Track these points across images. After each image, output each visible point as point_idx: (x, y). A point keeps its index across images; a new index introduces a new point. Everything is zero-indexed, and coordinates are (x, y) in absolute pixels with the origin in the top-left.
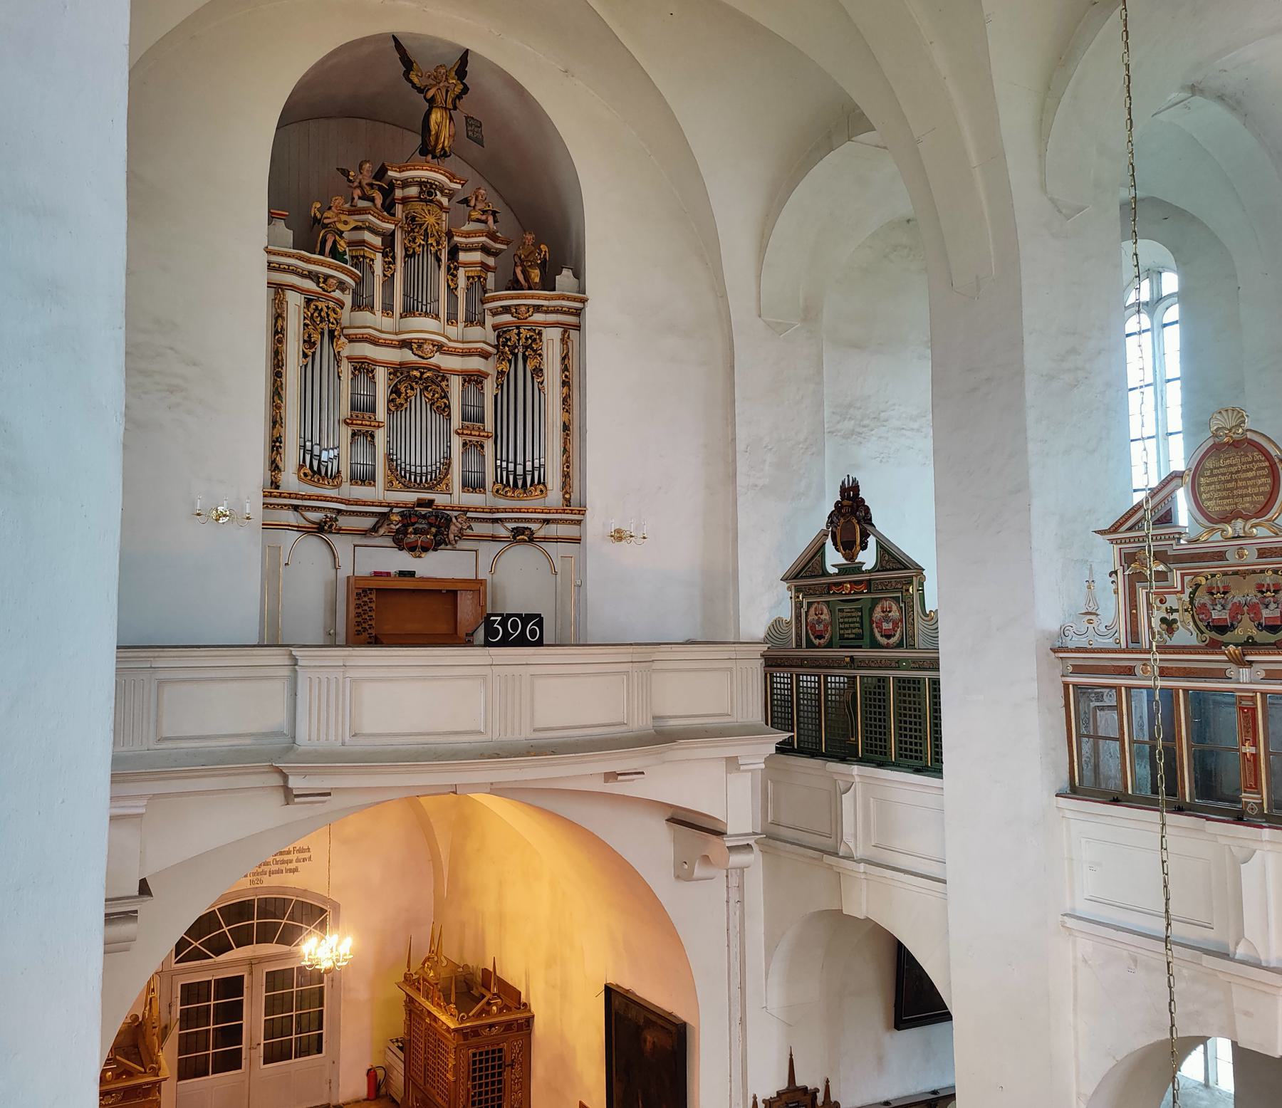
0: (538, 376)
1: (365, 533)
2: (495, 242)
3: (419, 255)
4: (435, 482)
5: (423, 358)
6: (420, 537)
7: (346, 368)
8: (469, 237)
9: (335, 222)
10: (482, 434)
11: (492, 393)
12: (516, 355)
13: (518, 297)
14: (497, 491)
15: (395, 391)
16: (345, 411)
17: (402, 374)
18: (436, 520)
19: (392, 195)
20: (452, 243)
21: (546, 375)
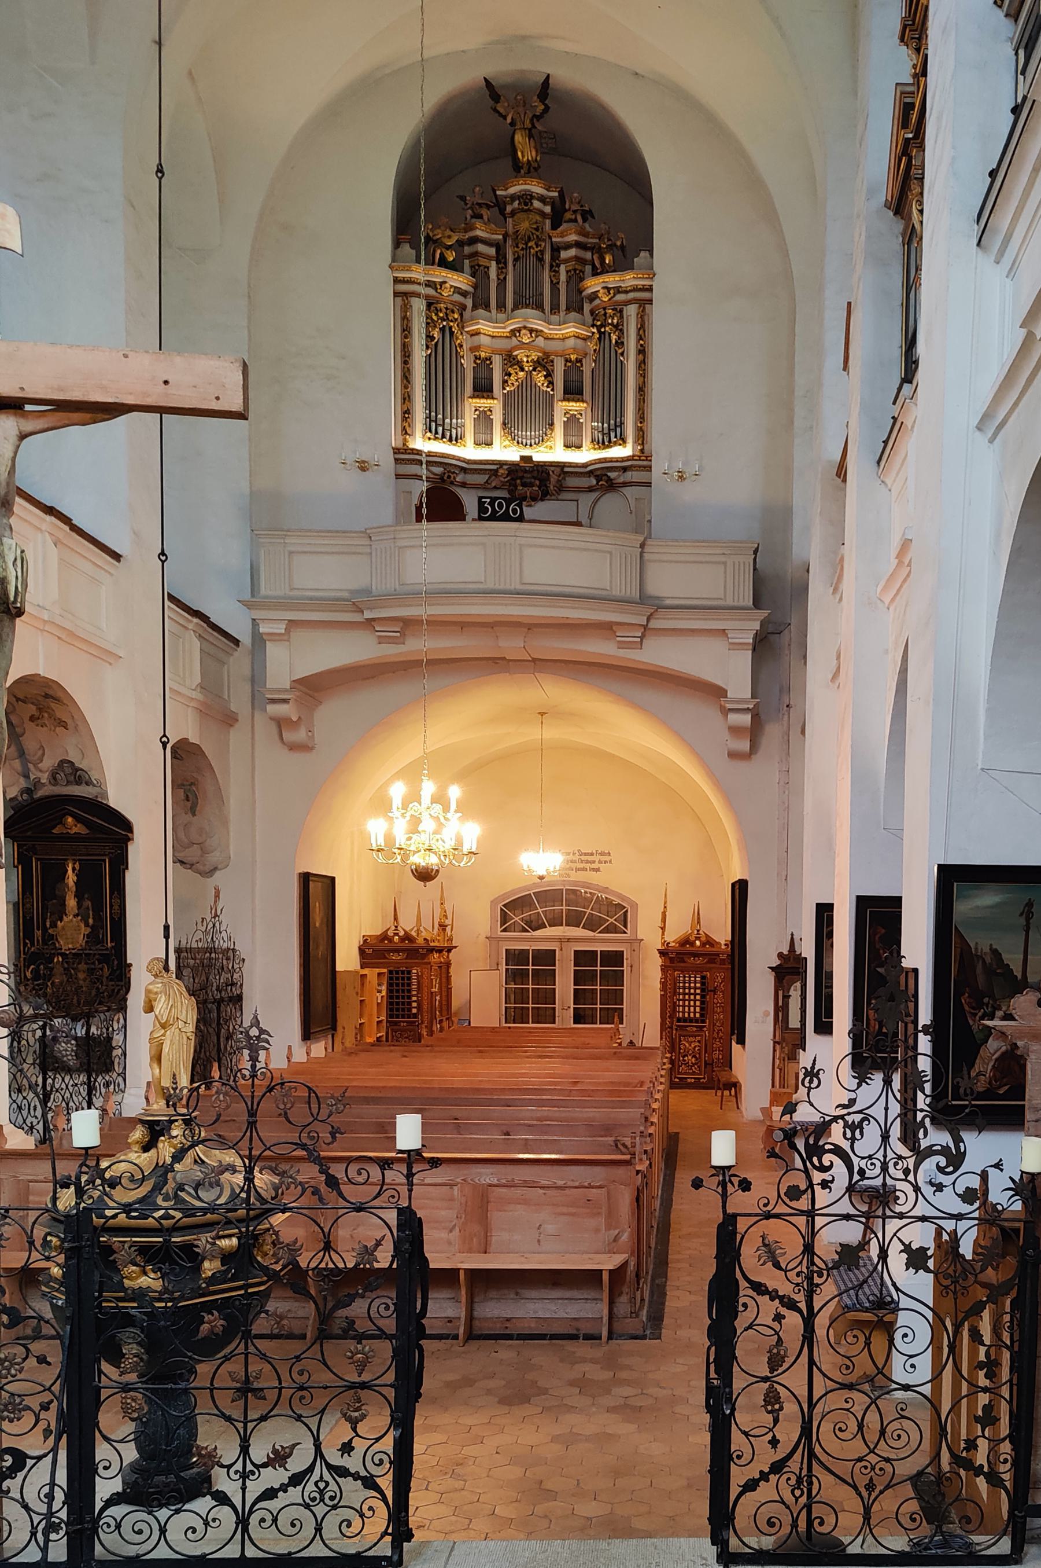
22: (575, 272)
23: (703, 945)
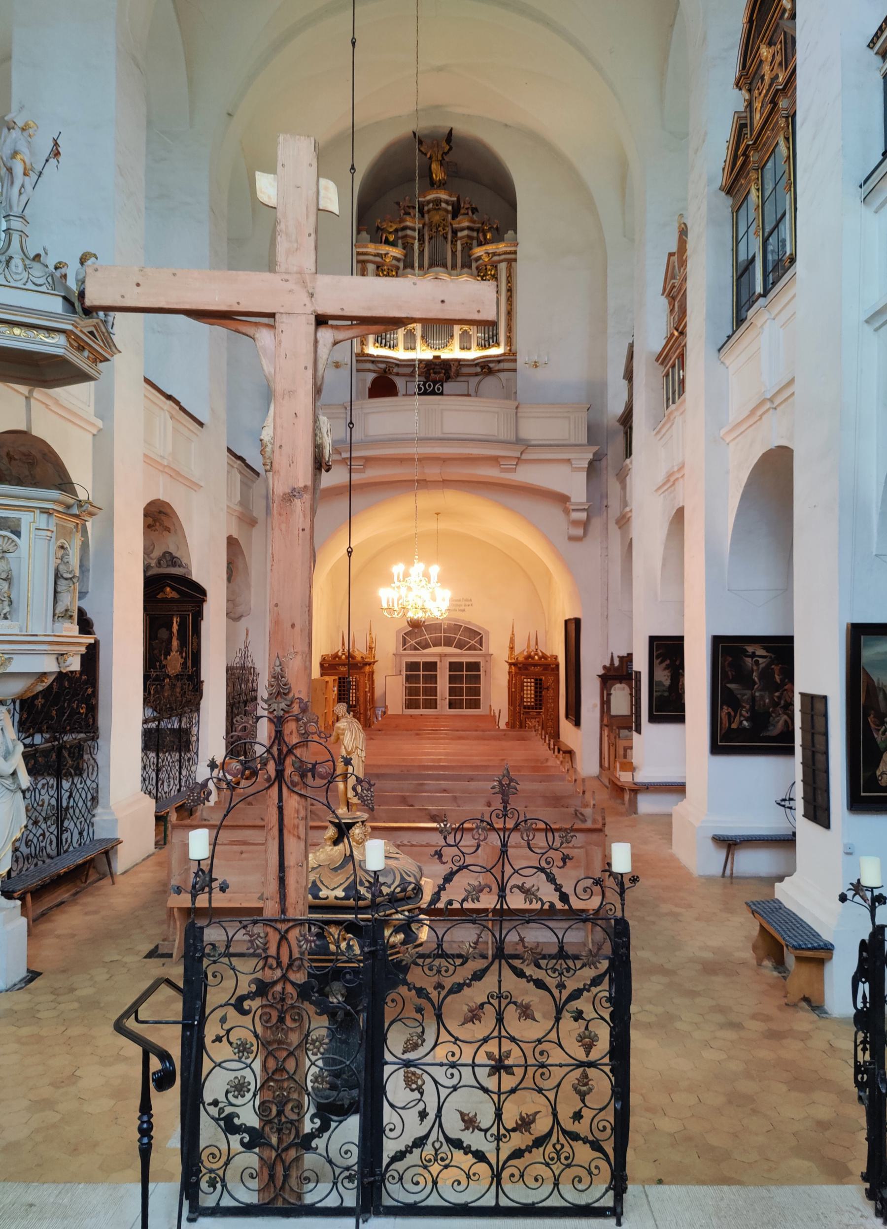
23: (540, 658)
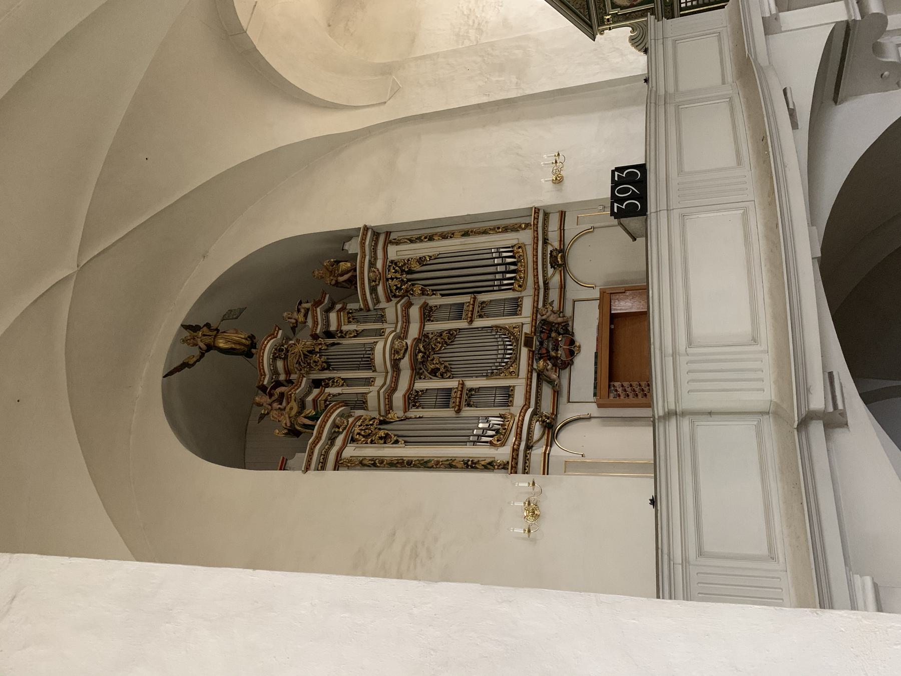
0: (425, 260)
1: (557, 393)
2: (323, 303)
3: (328, 359)
4: (512, 337)
5: (406, 350)
6: (561, 347)
7: (414, 413)
8: (317, 322)
9: (290, 418)
10: (472, 302)
11: (440, 298)
12: (409, 280)
13: (362, 279)
14: (520, 286)
15: (434, 373)
16: (449, 413)
17: (421, 369)
18: (544, 332)
19: (282, 382)
20: (321, 335)
21: (424, 254)
22: (351, 313)
